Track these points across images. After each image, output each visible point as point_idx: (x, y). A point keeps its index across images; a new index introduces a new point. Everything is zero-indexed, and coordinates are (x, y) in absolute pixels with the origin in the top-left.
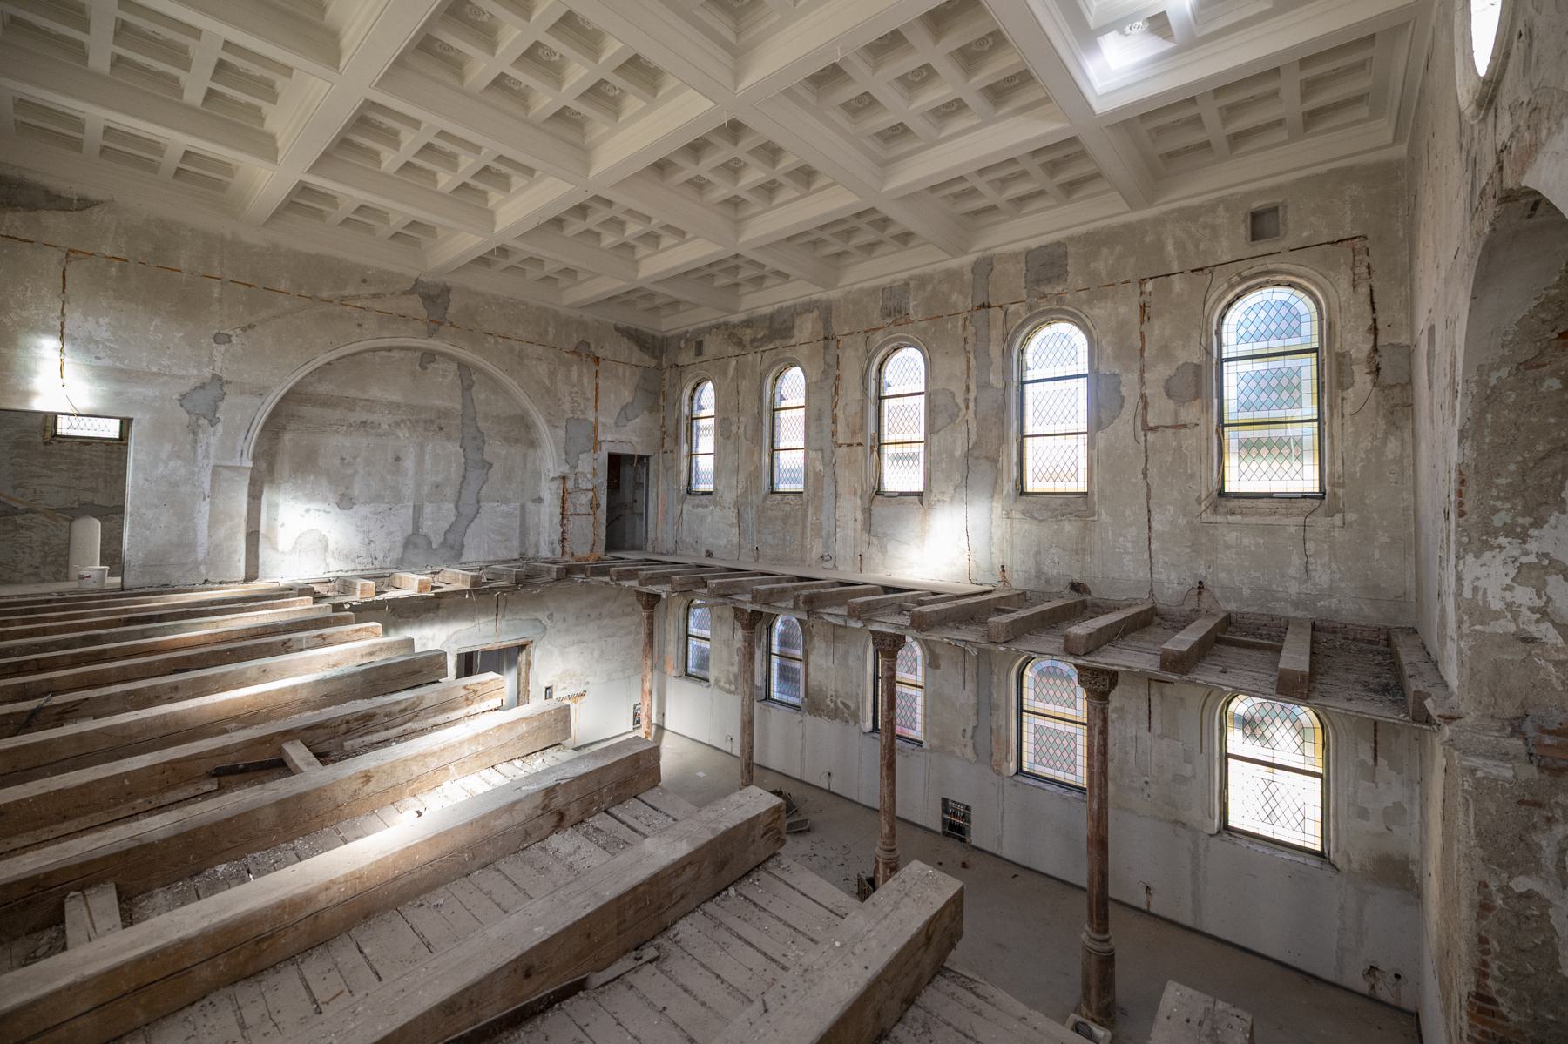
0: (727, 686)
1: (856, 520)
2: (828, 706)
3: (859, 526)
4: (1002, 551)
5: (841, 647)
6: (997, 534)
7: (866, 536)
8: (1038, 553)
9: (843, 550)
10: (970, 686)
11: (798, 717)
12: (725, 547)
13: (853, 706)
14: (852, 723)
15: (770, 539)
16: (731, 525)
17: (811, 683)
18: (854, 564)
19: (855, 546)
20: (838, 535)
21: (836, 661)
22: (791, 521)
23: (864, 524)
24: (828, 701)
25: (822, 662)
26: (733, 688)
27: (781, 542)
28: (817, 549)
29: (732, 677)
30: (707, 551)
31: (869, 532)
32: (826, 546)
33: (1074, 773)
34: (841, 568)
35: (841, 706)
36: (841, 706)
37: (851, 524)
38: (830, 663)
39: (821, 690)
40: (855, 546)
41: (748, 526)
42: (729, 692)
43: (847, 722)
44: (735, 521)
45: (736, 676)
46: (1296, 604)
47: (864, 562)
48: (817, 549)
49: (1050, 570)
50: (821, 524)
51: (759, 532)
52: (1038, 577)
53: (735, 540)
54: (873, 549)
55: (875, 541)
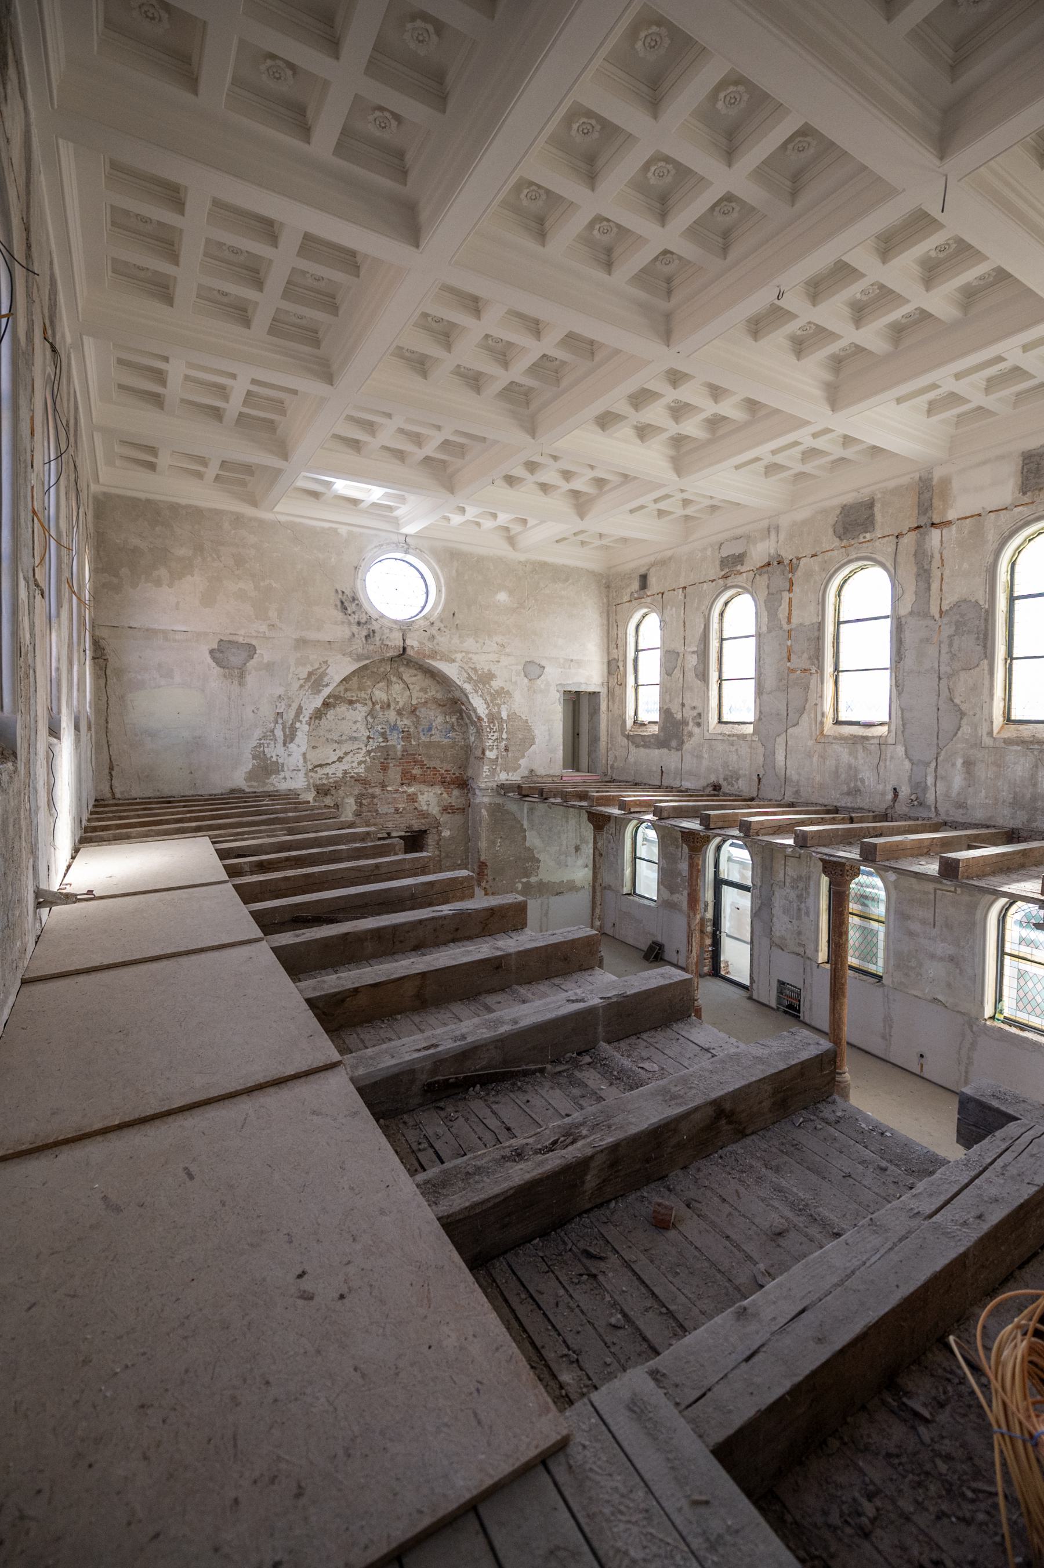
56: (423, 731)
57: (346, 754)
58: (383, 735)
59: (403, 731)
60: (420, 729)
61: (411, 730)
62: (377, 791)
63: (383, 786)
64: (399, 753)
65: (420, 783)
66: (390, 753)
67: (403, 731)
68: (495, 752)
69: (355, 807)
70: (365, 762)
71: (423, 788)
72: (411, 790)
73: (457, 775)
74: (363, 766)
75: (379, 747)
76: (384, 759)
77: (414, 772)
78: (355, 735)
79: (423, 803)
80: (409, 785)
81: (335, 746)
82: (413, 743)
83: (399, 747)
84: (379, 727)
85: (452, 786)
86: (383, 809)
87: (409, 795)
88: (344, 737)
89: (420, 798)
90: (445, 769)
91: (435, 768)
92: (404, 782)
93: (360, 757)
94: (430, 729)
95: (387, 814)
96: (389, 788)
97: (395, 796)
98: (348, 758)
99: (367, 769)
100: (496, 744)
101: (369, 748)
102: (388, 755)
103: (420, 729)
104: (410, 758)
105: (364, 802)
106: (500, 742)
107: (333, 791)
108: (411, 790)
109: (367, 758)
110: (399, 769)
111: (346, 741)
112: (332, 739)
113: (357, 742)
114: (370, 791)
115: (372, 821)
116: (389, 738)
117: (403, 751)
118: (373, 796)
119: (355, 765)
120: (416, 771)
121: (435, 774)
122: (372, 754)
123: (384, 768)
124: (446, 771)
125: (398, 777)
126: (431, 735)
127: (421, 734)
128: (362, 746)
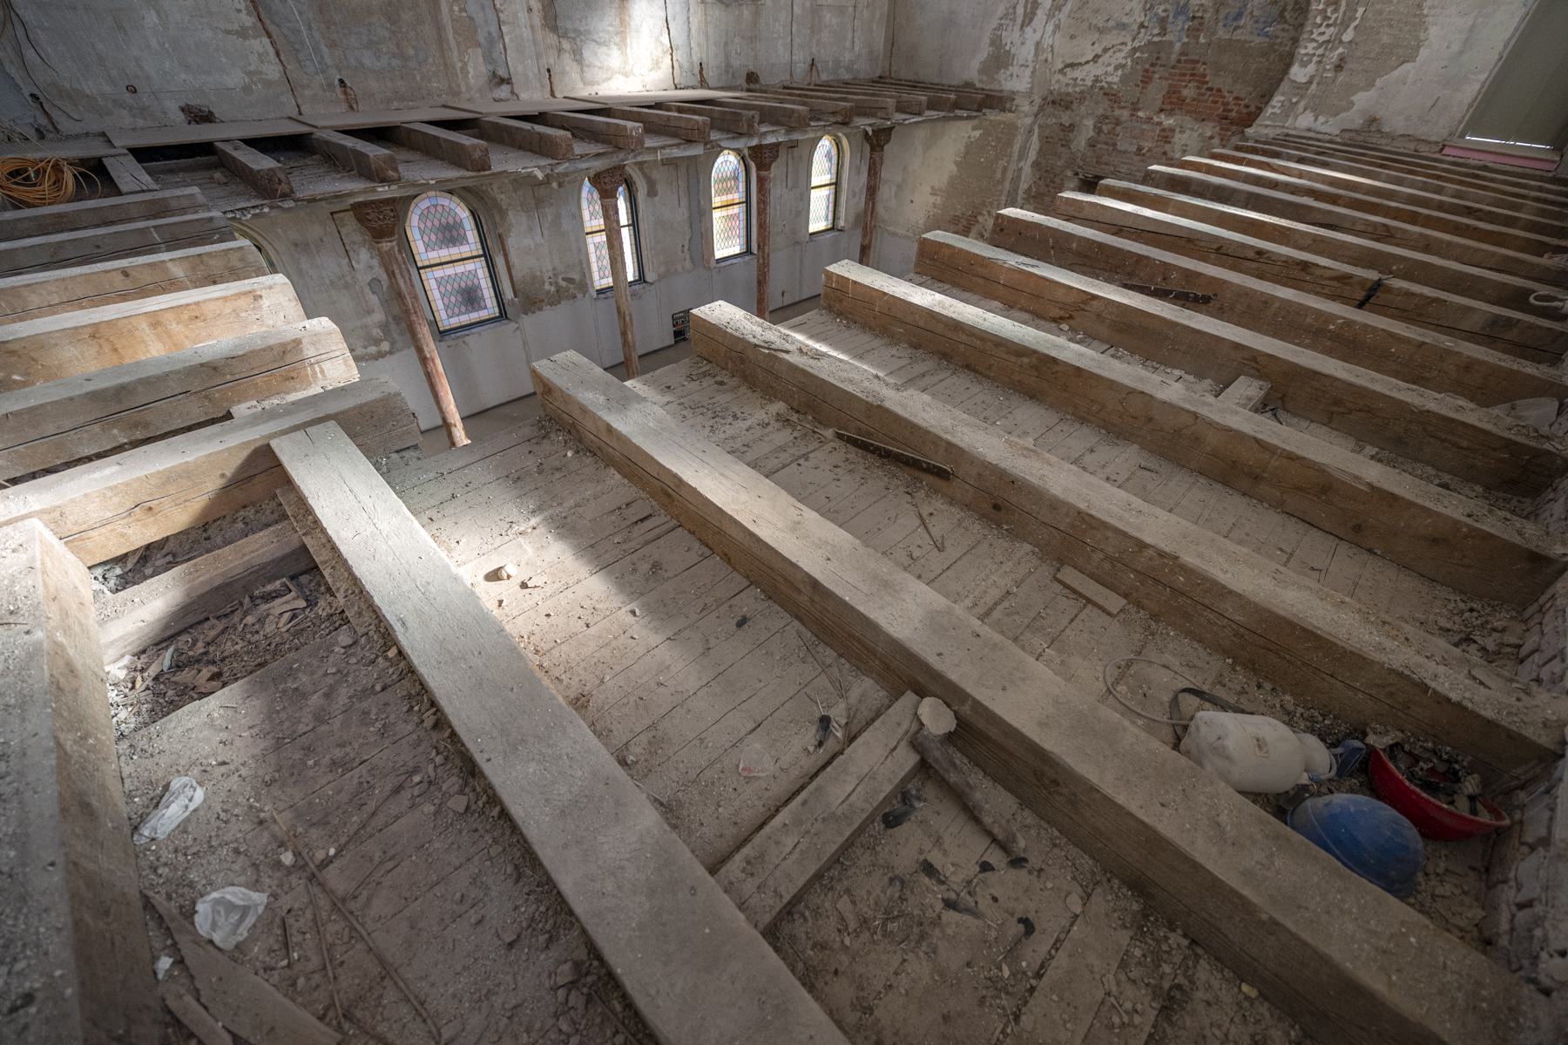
0: (373, 349)
1: (530, 10)
2: (548, 292)
3: (537, 20)
4: (699, 45)
5: (549, 212)
6: (695, 21)
7: (552, 39)
8: (726, 44)
9: (522, 67)
10: (684, 202)
11: (508, 328)
12: (247, 89)
13: (576, 276)
14: (580, 296)
15: (368, 59)
16: (242, 33)
17: (517, 274)
18: (542, 86)
19: (539, 56)
20: (507, 40)
21: (546, 232)
22: (407, 16)
23: (545, 18)
24: (547, 287)
25: (527, 242)
26: (385, 346)
27: (396, 63)
28: (475, 68)
29: (376, 332)
30: (186, 110)
31: (554, 29)
32: (489, 58)
33: (601, 278)
34: (524, 96)
35: (564, 284)
36: (564, 284)
37: (523, 16)
38: (538, 238)
39: (534, 277)
40: (539, 56)
41: (297, 32)
42: (381, 355)
43: (574, 297)
44: (249, 21)
45: (384, 327)
46: (848, 69)
47: (555, 79)
48: (475, 68)
49: (735, 63)
50: (471, 18)
51: (333, 45)
52: (727, 72)
53: (273, 71)
54: (567, 59)
55: (566, 45)
56: (1226, 18)
57: (1105, 50)
58: (1163, 22)
59: (1194, 18)
60: (1221, 16)
61: (1207, 16)
62: (1125, 114)
63: (1135, 108)
64: (1174, 57)
65: (1188, 112)
66: (1163, 55)
67: (1194, 18)
68: (1311, 68)
69: (1091, 133)
70: (1123, 66)
71: (1188, 121)
72: (1169, 122)
73: (1253, 108)
74: (1120, 72)
75: (1150, 43)
76: (1150, 63)
77: (1185, 92)
78: (1125, 20)
79: (1177, 147)
80: (1170, 113)
81: (1097, 35)
82: (1202, 40)
83: (1178, 45)
84: (1162, 7)
85: (1234, 128)
86: (1123, 145)
87: (1164, 130)
88: (1111, 23)
89: (1177, 136)
90: (1235, 94)
91: (1219, 90)
92: (1165, 107)
93: (1119, 58)
94: (1239, 15)
95: (1125, 152)
96: (1141, 114)
97: (1144, 127)
98: (1105, 58)
99: (1124, 79)
100: (1320, 51)
101: (1136, 44)
102: (1158, 58)
103: (1221, 16)
104: (1189, 67)
105: (1104, 127)
106: (1334, 49)
107: (1075, 106)
108: (1169, 122)
109: (1129, 60)
110: (1165, 83)
111: (1110, 30)
112: (1095, 26)
113: (1124, 33)
114: (1117, 112)
115: (1105, 158)
116: (1169, 28)
117: (1183, 54)
118: (1118, 122)
119: (1110, 69)
120: (1189, 92)
121: (1216, 102)
122: (1138, 54)
123: (1146, 80)
124: (1237, 98)
125: (1160, 96)
126: (1236, 28)
127: (1221, 24)
128: (1128, 39)
